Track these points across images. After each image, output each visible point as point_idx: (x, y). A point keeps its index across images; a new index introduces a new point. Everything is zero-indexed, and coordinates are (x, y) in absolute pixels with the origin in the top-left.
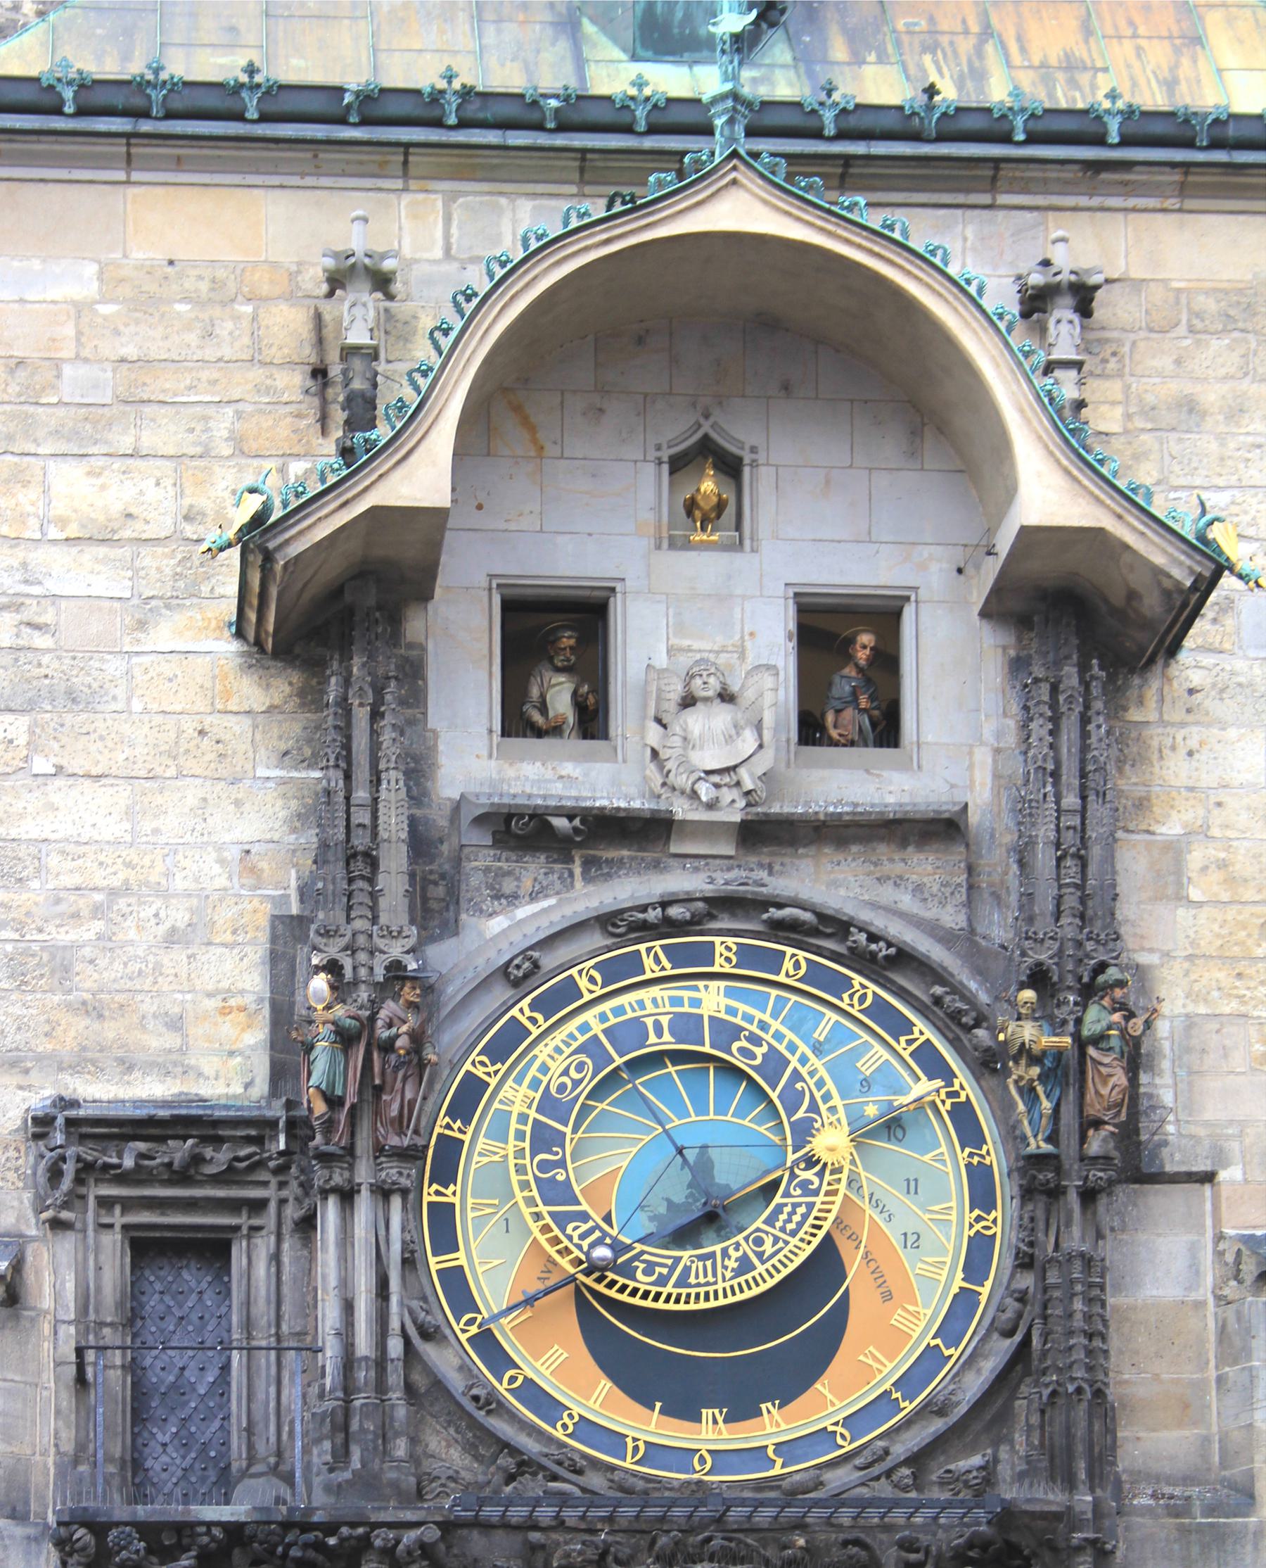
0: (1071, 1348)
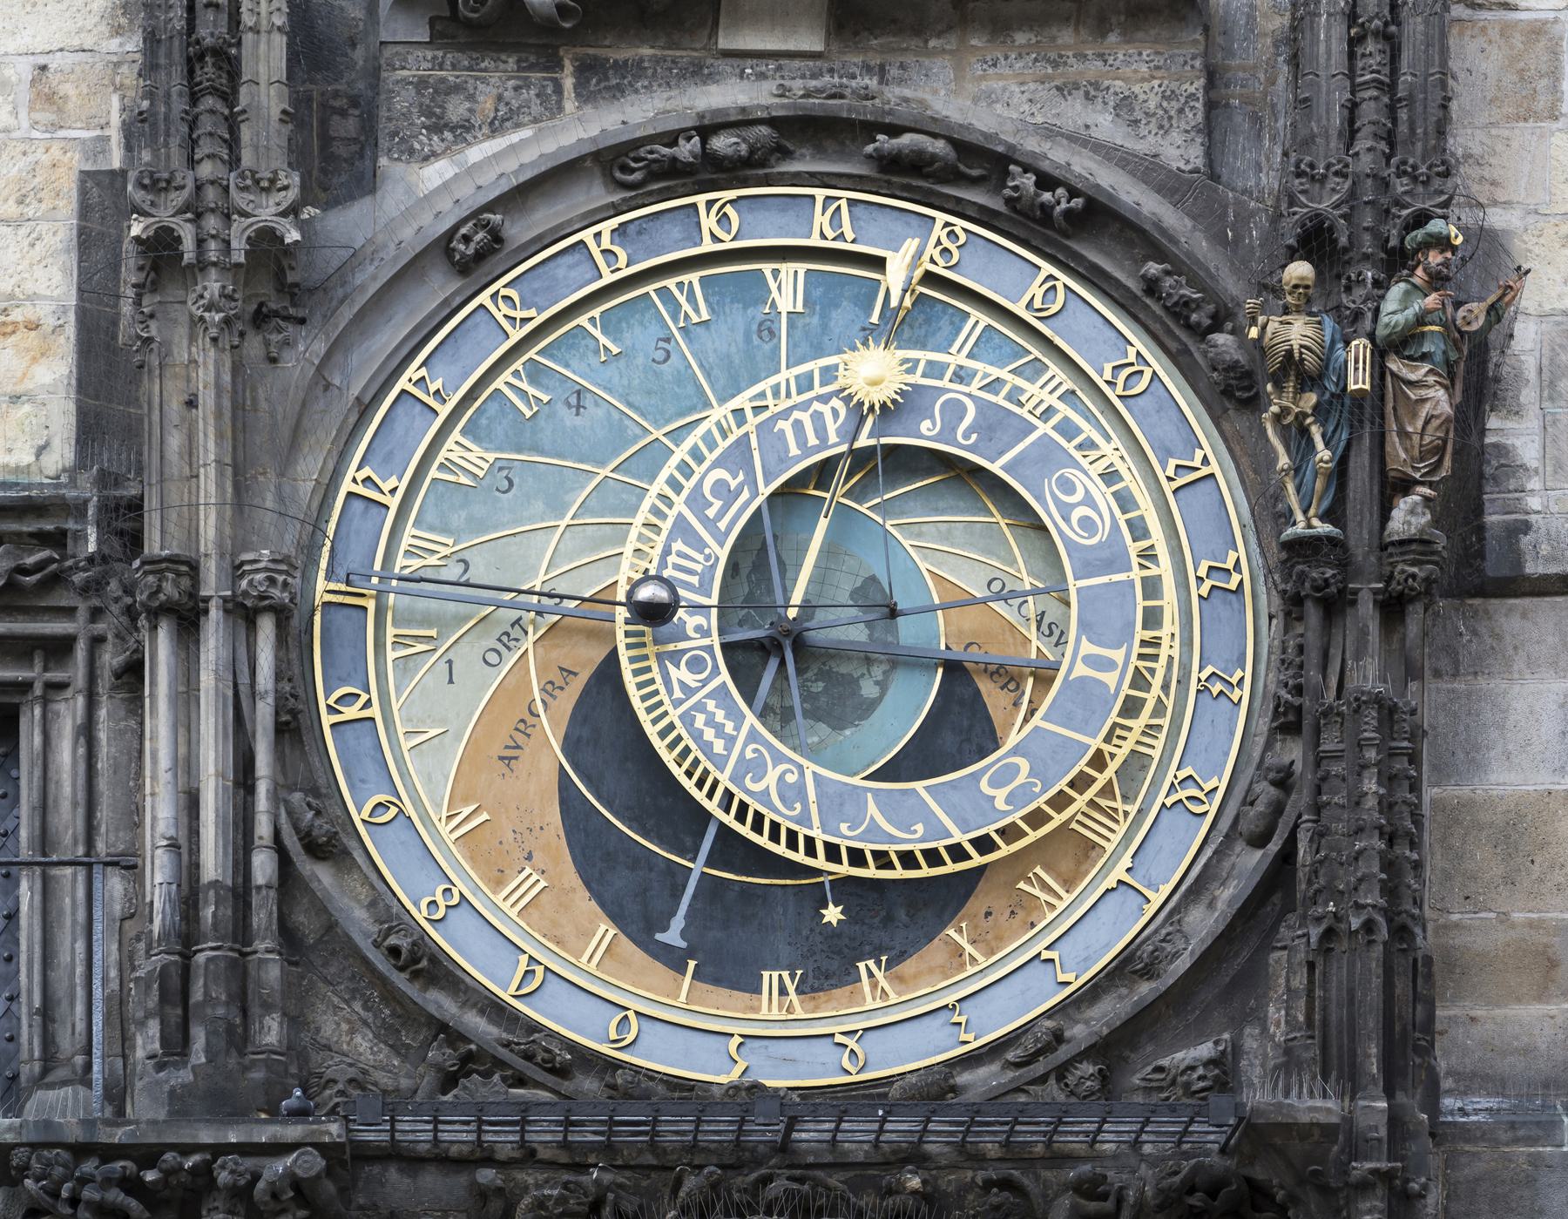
0: (1360, 853)
